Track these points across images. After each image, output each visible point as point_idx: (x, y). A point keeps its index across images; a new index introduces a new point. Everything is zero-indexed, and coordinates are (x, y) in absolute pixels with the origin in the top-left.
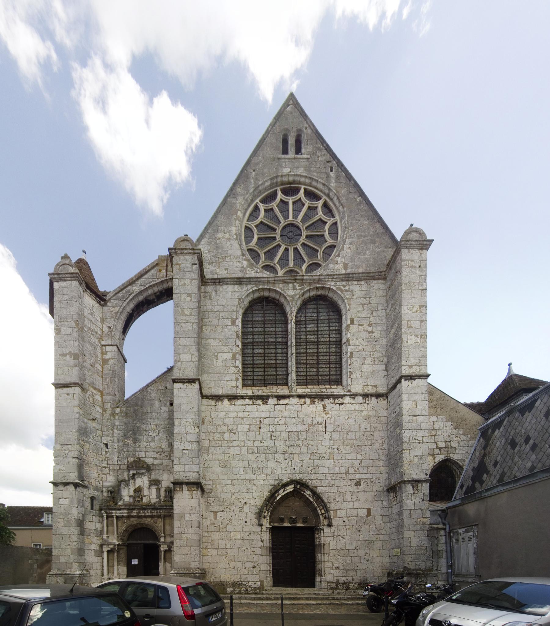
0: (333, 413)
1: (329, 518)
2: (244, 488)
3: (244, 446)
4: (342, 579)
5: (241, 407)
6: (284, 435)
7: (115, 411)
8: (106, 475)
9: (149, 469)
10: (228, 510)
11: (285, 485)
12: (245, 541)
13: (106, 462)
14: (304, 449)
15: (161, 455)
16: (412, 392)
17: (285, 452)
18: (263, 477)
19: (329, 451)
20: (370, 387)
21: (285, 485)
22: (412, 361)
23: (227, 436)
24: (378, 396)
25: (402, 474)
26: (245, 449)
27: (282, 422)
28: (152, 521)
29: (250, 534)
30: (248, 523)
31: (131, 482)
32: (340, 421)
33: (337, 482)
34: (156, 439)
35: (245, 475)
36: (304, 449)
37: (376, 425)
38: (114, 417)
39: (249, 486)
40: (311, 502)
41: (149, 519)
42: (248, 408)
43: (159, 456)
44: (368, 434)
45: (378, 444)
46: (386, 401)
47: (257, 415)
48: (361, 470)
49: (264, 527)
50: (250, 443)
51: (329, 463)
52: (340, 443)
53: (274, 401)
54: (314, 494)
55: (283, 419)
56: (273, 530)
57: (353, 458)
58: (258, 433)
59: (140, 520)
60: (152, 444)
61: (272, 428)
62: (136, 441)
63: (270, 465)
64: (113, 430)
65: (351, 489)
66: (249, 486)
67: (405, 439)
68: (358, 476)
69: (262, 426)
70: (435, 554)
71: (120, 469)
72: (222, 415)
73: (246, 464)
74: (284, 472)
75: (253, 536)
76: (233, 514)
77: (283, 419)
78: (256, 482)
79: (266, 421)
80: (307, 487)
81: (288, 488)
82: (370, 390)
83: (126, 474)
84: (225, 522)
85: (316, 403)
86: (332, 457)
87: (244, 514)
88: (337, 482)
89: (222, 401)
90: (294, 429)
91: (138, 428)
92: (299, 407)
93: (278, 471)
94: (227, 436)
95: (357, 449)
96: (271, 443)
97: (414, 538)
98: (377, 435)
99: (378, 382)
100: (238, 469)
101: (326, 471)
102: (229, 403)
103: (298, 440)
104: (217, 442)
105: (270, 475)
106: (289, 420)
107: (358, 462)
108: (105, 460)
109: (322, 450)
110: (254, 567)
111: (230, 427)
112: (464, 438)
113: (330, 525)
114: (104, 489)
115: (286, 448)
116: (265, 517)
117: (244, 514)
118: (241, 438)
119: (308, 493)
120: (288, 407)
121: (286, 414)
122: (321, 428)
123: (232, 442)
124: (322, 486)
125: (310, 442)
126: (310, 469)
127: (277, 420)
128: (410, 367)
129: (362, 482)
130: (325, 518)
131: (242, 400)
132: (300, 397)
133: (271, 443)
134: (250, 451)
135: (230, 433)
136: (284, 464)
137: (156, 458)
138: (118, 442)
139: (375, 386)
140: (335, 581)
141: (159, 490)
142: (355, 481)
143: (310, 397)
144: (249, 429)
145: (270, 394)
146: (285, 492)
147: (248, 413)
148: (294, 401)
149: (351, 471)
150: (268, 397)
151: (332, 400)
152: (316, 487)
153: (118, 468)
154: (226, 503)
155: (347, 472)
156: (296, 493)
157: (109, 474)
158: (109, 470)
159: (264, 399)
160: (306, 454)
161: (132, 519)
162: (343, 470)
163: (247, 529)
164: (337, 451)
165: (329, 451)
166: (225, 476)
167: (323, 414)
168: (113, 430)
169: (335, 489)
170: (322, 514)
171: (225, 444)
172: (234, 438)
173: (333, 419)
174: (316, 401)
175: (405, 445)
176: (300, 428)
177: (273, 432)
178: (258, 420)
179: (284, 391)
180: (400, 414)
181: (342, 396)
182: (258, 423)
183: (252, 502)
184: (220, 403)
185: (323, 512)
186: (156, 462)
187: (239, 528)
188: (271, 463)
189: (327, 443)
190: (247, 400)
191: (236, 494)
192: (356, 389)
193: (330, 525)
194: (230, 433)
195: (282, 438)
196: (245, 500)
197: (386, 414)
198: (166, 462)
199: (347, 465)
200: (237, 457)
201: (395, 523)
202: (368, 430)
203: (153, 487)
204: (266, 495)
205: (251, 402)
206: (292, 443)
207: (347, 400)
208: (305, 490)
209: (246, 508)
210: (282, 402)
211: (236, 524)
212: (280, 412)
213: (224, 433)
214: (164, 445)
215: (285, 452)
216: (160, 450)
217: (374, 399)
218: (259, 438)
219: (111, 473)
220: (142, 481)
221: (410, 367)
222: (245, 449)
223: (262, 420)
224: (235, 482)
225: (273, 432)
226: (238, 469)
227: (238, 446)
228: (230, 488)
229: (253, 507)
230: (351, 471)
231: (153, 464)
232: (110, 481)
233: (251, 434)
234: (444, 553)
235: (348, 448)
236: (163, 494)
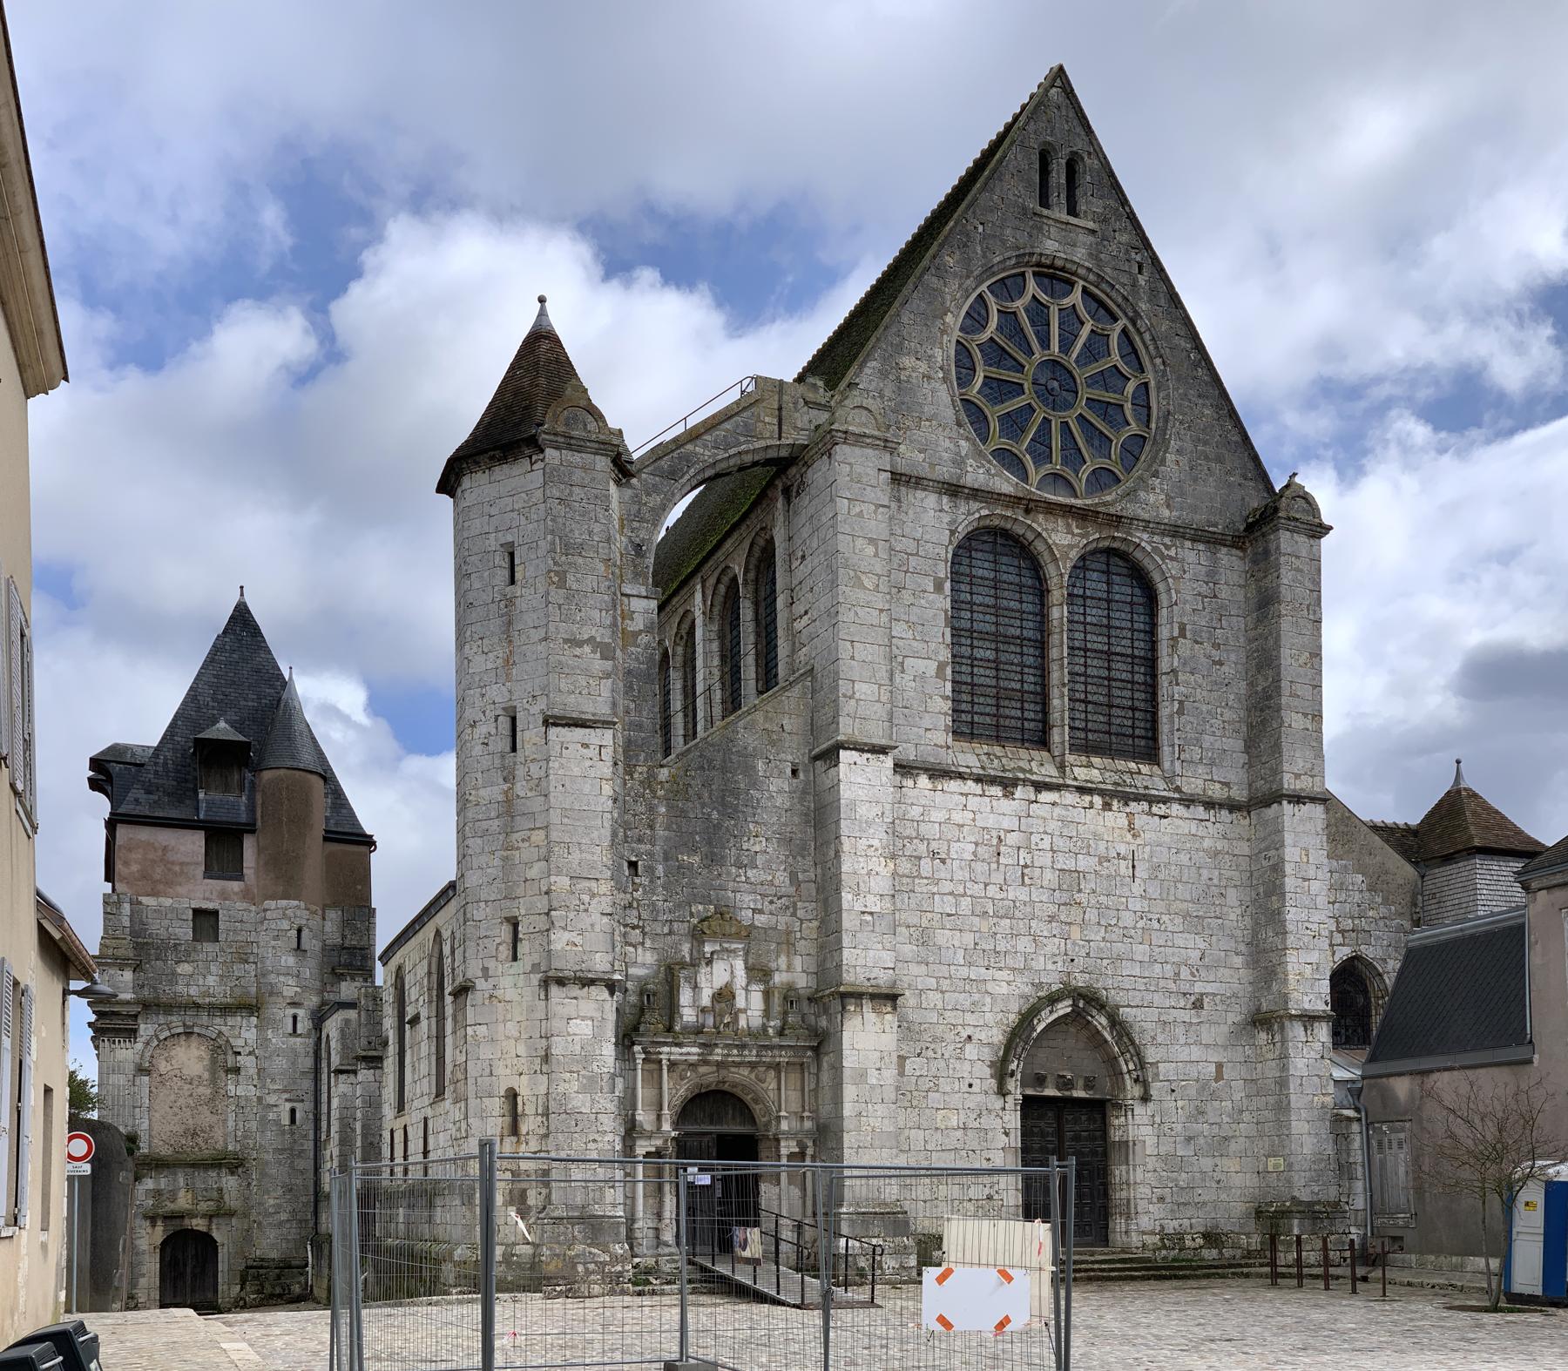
0: (1148, 835)
1: (1145, 1085)
2: (964, 1000)
3: (965, 895)
4: (1172, 1226)
5: (957, 797)
6: (1050, 877)
7: (654, 776)
8: (634, 946)
9: (747, 934)
10: (930, 1053)
11: (1053, 999)
12: (969, 1132)
13: (635, 913)
14: (1092, 915)
15: (771, 902)
16: (1301, 828)
17: (1052, 919)
18: (1005, 975)
19: (1141, 924)
20: (1218, 786)
21: (1053, 999)
22: (1300, 765)
23: (926, 865)
24: (1233, 806)
25: (1285, 998)
26: (966, 903)
27: (1046, 845)
28: (753, 1076)
29: (979, 1116)
30: (974, 1089)
31: (704, 970)
32: (1163, 856)
33: (1158, 999)
34: (760, 860)
35: (966, 969)
36: (1092, 915)
37: (1229, 874)
38: (653, 792)
39: (976, 997)
40: (1106, 1041)
41: (745, 1071)
42: (973, 802)
43: (767, 907)
44: (1215, 891)
45: (1233, 917)
46: (1247, 821)
47: (991, 822)
48: (1203, 973)
49: (1009, 1099)
50: (977, 889)
51: (1141, 951)
52: (1160, 906)
53: (1030, 792)
54: (1115, 1022)
55: (1047, 839)
56: (1029, 1106)
57: (1191, 945)
58: (994, 866)
59: (723, 1072)
60: (750, 874)
61: (1024, 857)
62: (713, 860)
63: (1020, 948)
64: (651, 827)
65: (1186, 1016)
66: (976, 997)
67: (1290, 927)
68: (1199, 988)
69: (1002, 849)
70: (1344, 1170)
71: (671, 933)
72: (915, 812)
73: (969, 939)
74: (1050, 966)
75: (986, 1122)
76: (942, 1064)
77: (1047, 839)
78: (990, 987)
79: (1012, 839)
80: (1102, 1007)
81: (1060, 1006)
82: (1216, 792)
83: (686, 948)
84: (925, 1084)
85: (1115, 808)
86: (1147, 937)
87: (967, 1066)
88: (1158, 999)
89: (915, 777)
90: (1070, 865)
91: (718, 827)
92: (1079, 815)
93: (1039, 963)
94: (926, 865)
95: (1194, 923)
96: (1021, 894)
97: (1307, 1136)
98: (1232, 896)
99: (1231, 777)
100: (951, 951)
101: (1137, 972)
102: (930, 786)
103: (1080, 891)
104: (905, 880)
105: (1021, 971)
106: (1060, 843)
107: (1198, 954)
108: (630, 906)
109: (1127, 919)
110: (990, 1198)
111: (934, 845)
112: (1383, 910)
113: (1145, 1098)
114: (629, 985)
115: (1053, 909)
116: (1012, 1075)
117: (967, 1066)
118: (959, 875)
119: (1101, 1021)
120: (1057, 810)
121: (1053, 826)
122: (1124, 868)
123: (937, 882)
124: (1129, 1006)
125: (1103, 899)
126: (1105, 962)
127: (1035, 838)
128: (1297, 776)
129: (1206, 1000)
130: (1136, 1081)
131: (959, 782)
132: (1082, 790)
133: (1021, 894)
134: (978, 910)
135: (933, 859)
136: (1053, 945)
137: (761, 912)
138: (666, 859)
139: (1227, 784)
140: (1158, 1229)
141: (767, 995)
142: (1193, 998)
143: (1102, 793)
144: (975, 854)
145: (1021, 776)
146: (1055, 1016)
147: (971, 815)
148: (1070, 798)
149: (1185, 973)
150: (1014, 783)
151: (1145, 805)
152: (1118, 1007)
153: (666, 930)
154: (926, 1037)
155: (1177, 974)
156: (1077, 1018)
157: (643, 944)
158: (644, 934)
159: (1008, 785)
160: (1096, 928)
161: (702, 1070)
162: (1169, 970)
163: (973, 1101)
164: (1156, 926)
165: (1141, 924)
166: (924, 967)
167: (1129, 837)
168: (651, 827)
169: (1153, 1014)
170: (1129, 1072)
171: (921, 886)
172: (943, 873)
173: (1148, 849)
174: (1115, 803)
175: (1291, 940)
176: (1084, 863)
177: (1026, 866)
178: (994, 834)
179: (1049, 772)
180: (1278, 869)
181: (1165, 800)
182: (995, 841)
183: (982, 1035)
184: (910, 783)
185: (1131, 1066)
186: (761, 920)
187: (955, 1100)
188: (1024, 944)
189: (1136, 905)
190: (970, 783)
191: (948, 1014)
192: (1192, 784)
193: (1145, 1098)
194: (933, 859)
195: (1045, 883)
196: (969, 1031)
197: (1247, 851)
198: (783, 921)
199: (1176, 959)
200: (948, 922)
201: (1271, 1100)
202: (1216, 881)
203: (754, 987)
204: (1013, 1018)
205: (977, 788)
206: (1065, 897)
207: (1176, 809)
208: (1094, 1012)
209: (971, 1051)
210: (1046, 796)
211: (948, 1089)
212: (1040, 822)
213: (920, 858)
214: (782, 877)
215: (1052, 919)
216: (772, 891)
217: (1224, 812)
218: (998, 878)
219: (648, 944)
220: (725, 971)
221: (1297, 776)
222: (966, 903)
223: (1002, 834)
224: (945, 984)
225: (1026, 866)
226: (951, 951)
227: (951, 893)
228: (934, 998)
229: (986, 1050)
230: (1185, 973)
231: (752, 926)
232: (644, 962)
233: (980, 867)
234: (1360, 1169)
235: (1179, 920)
236: (777, 1007)
